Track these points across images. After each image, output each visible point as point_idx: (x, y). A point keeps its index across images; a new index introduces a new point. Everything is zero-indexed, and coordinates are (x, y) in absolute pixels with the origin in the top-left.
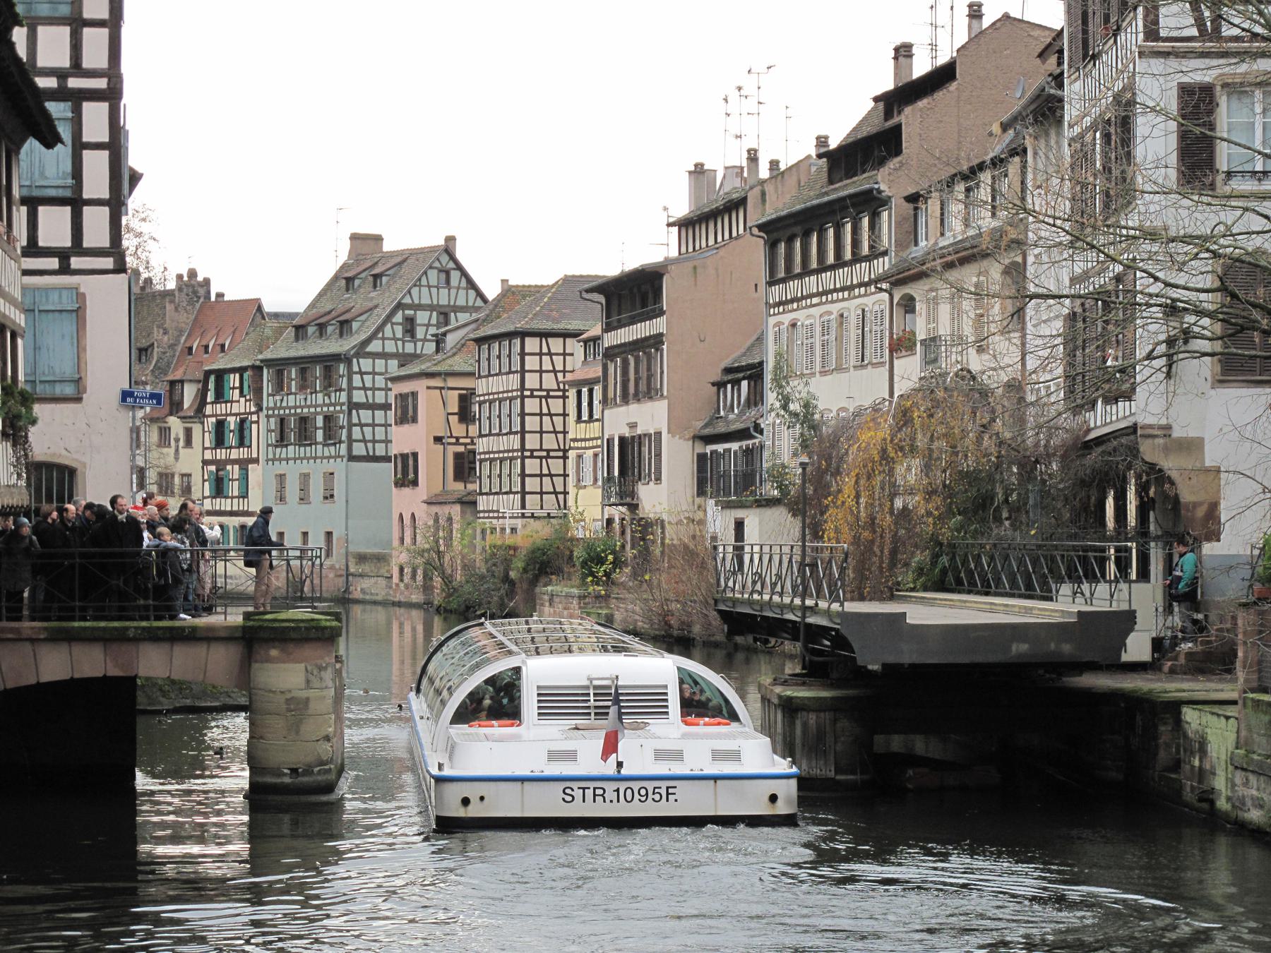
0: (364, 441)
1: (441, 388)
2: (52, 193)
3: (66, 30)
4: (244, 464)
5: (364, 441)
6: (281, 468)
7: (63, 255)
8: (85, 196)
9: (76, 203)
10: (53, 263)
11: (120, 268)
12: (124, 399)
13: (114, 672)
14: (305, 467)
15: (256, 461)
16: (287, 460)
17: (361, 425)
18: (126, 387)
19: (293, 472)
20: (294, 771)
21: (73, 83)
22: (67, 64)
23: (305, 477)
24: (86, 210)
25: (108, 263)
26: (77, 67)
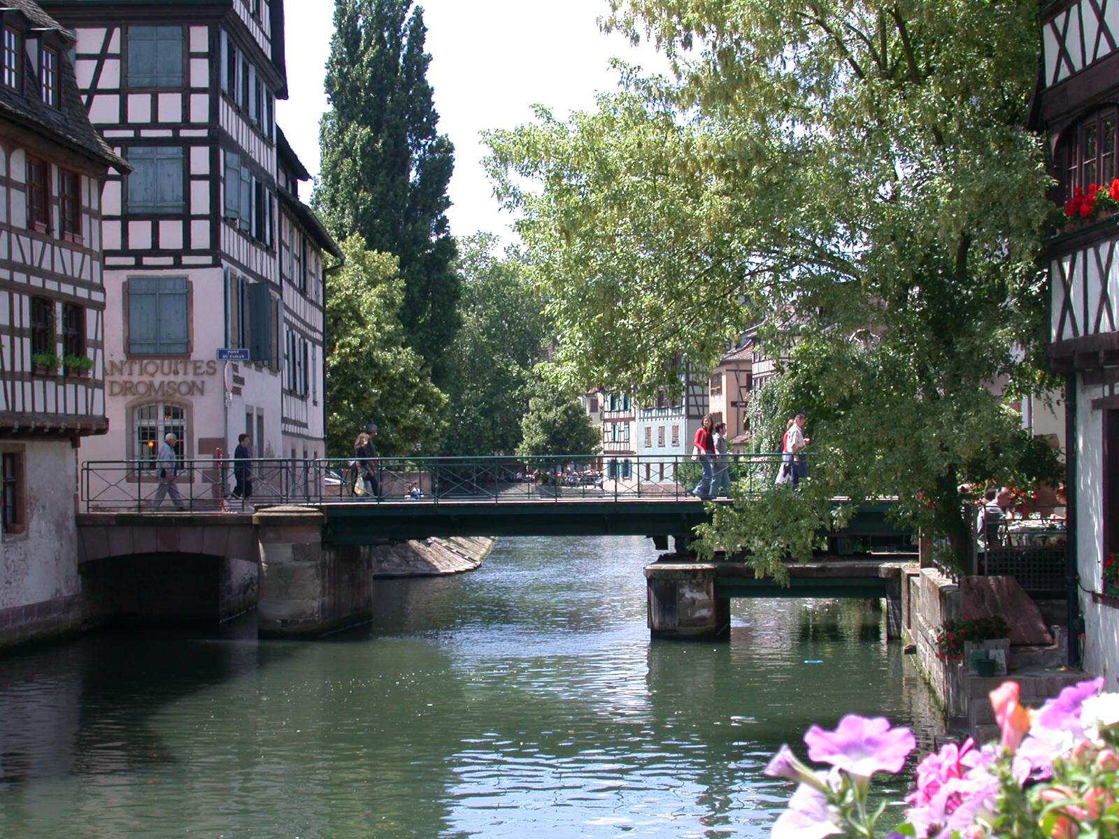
0: (697, 406)
1: (735, 371)
2: (170, 211)
3: (178, 97)
4: (627, 421)
5: (697, 406)
6: (648, 423)
7: (176, 254)
8: (193, 212)
9: (187, 218)
10: (169, 261)
11: (216, 264)
12: (221, 357)
13: (163, 549)
14: (661, 422)
15: (634, 419)
16: (652, 418)
17: (695, 396)
18: (222, 346)
19: (655, 425)
20: (284, 621)
21: (184, 133)
22: (178, 119)
23: (662, 429)
24: (193, 222)
25: (208, 260)
26: (186, 123)
